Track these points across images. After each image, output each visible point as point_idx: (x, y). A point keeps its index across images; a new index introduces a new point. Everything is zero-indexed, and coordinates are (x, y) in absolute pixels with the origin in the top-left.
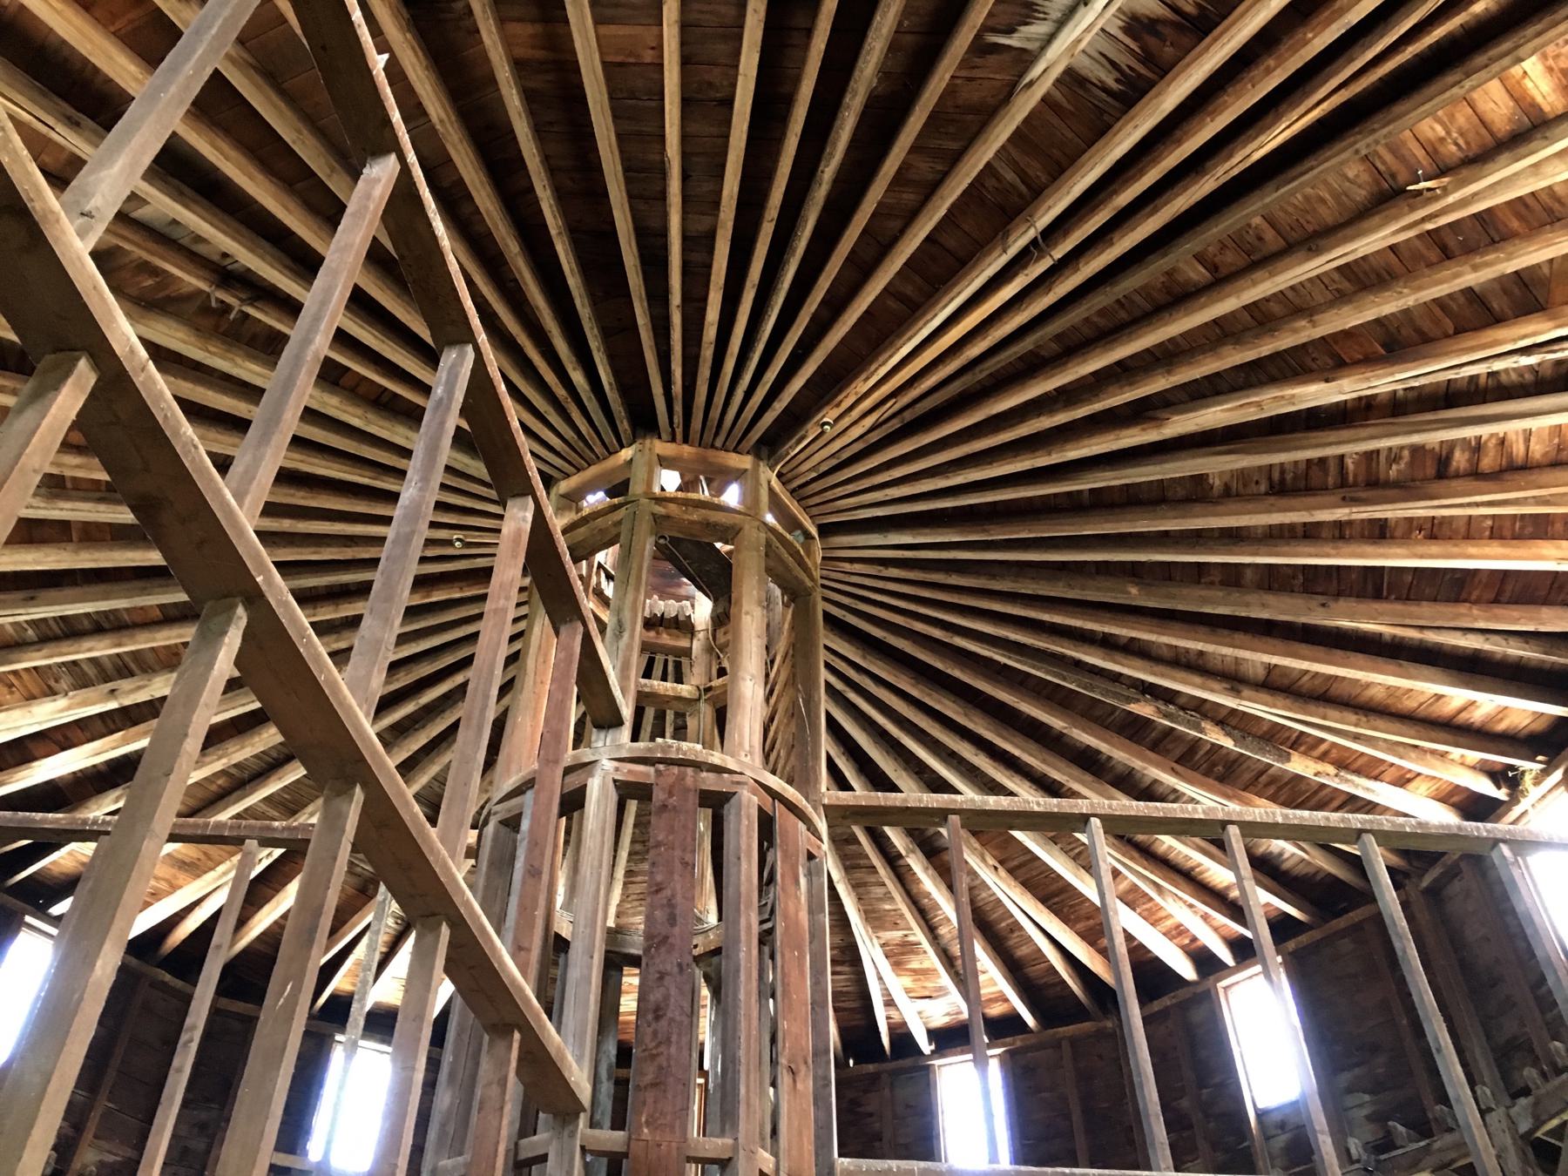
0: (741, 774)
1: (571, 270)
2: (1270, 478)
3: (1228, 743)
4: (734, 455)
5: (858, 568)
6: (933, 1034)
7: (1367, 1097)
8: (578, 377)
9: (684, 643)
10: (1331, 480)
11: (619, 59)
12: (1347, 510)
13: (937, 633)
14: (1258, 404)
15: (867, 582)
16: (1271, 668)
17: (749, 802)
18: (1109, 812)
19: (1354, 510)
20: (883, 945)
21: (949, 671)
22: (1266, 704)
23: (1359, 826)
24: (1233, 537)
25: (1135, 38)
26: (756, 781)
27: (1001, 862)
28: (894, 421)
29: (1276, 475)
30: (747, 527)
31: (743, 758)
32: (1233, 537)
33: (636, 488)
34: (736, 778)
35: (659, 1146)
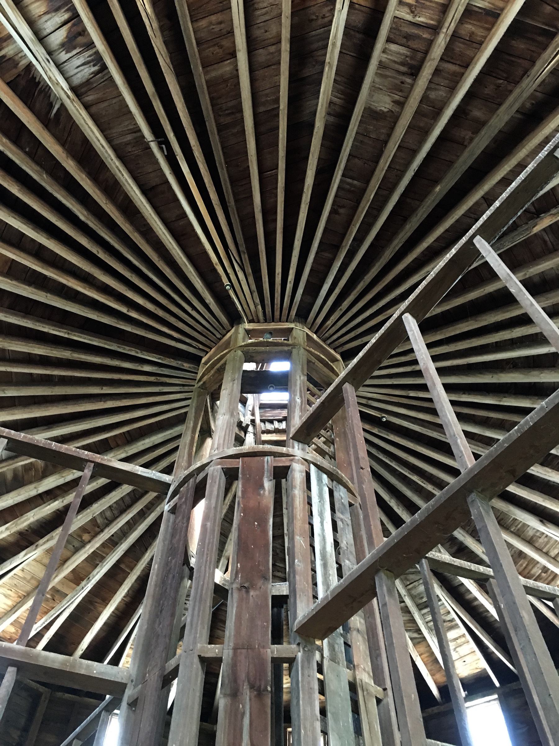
0: (211, 461)
1: (90, 340)
2: (404, 74)
5: (333, 318)
8: (147, 368)
10: (426, 36)
11: (7, 268)
12: (442, 36)
19: (444, 30)
25: (75, 48)
28: (242, 256)
29: (403, 69)
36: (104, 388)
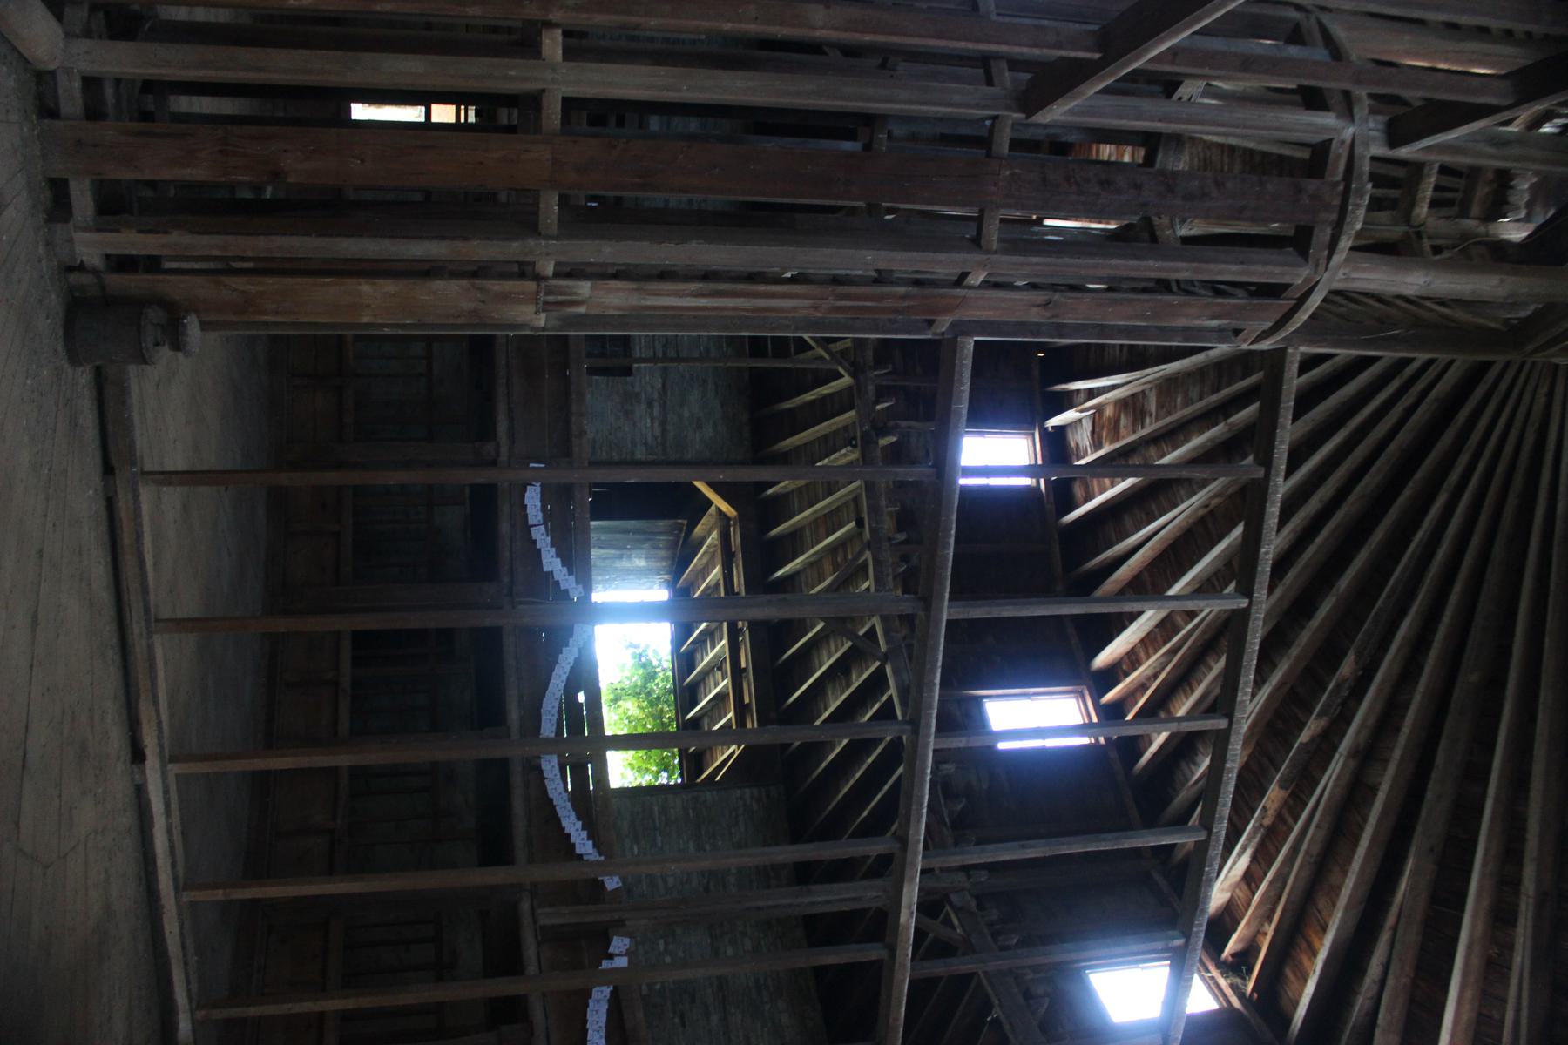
0: (1326, 269)
3: (1304, 737)
6: (1061, 430)
7: (985, 786)
9: (1475, 210)
13: (1454, 477)
15: (1523, 410)
16: (1374, 790)
17: (1299, 276)
18: (1253, 616)
20: (1143, 392)
21: (1411, 484)
22: (1338, 778)
23: (1215, 830)
24: (1518, 783)
26: (1318, 282)
27: (1212, 512)
31: (1342, 271)
32: (1518, 783)
34: (1323, 262)
35: (995, 185)
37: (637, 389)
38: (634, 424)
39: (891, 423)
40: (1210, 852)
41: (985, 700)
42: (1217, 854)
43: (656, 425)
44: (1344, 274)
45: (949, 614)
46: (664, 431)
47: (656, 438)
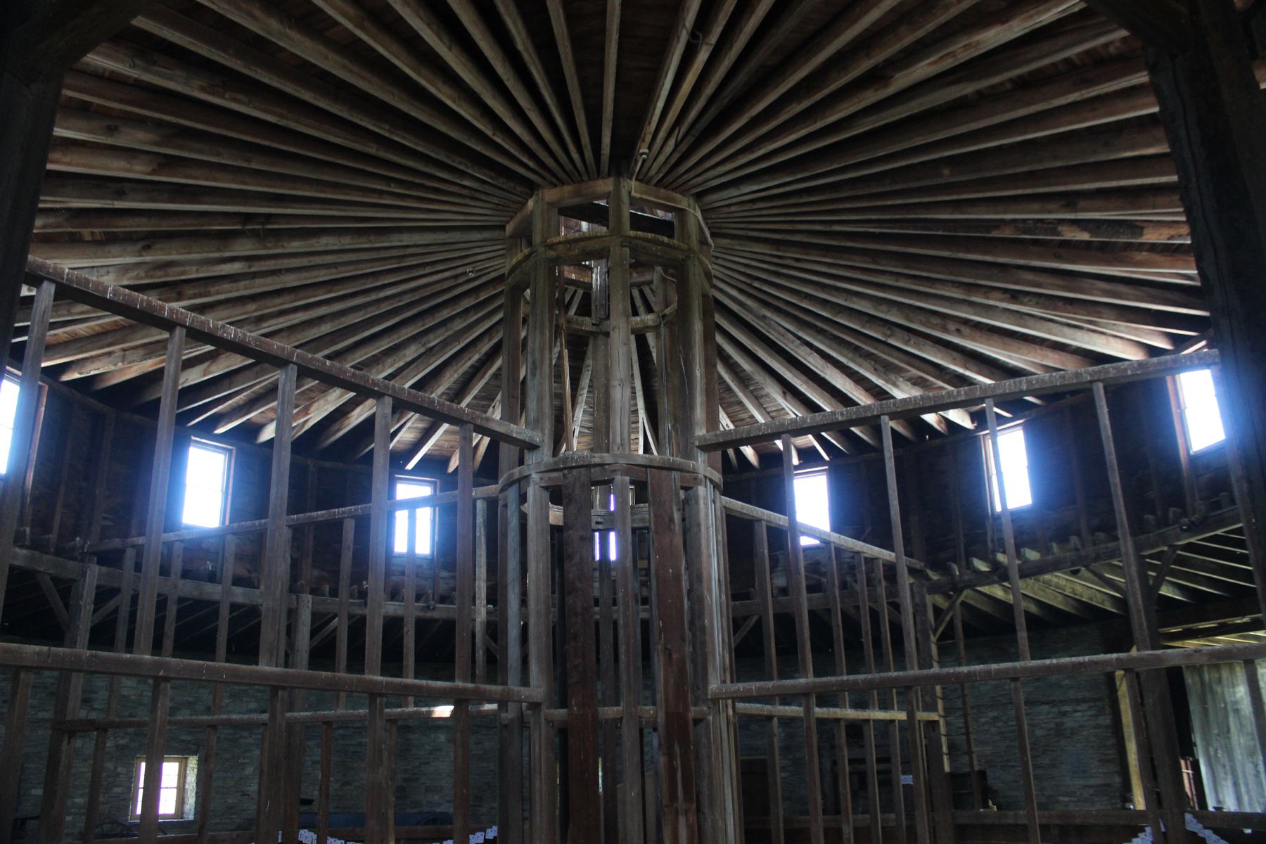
1: (415, 144)
4: (600, 182)
5: (733, 209)
8: (466, 183)
9: (647, 277)
13: (818, 227)
14: (953, 54)
18: (894, 409)
23: (1089, 378)
28: (689, 138)
30: (612, 249)
33: (537, 239)
36: (393, 185)
37: (1053, 725)
38: (1081, 726)
39: (991, 557)
40: (1111, 375)
41: (1191, 453)
42: (1114, 368)
43: (1079, 708)
44: (619, 448)
45: (912, 668)
46: (1084, 701)
47: (1091, 707)
